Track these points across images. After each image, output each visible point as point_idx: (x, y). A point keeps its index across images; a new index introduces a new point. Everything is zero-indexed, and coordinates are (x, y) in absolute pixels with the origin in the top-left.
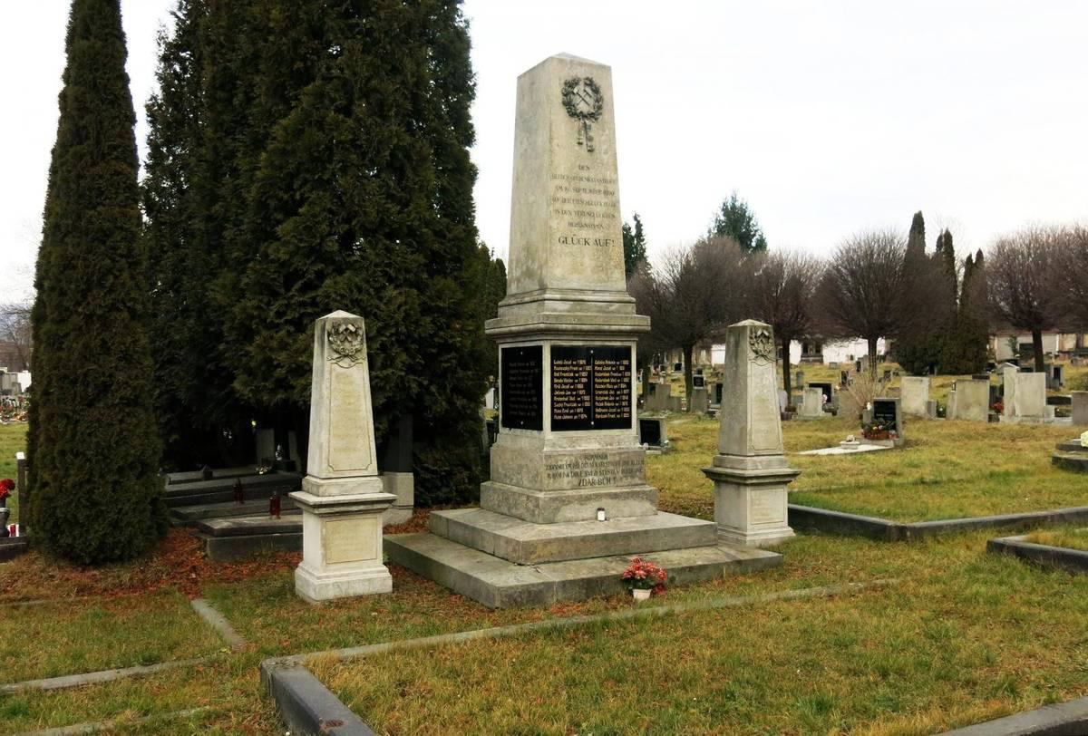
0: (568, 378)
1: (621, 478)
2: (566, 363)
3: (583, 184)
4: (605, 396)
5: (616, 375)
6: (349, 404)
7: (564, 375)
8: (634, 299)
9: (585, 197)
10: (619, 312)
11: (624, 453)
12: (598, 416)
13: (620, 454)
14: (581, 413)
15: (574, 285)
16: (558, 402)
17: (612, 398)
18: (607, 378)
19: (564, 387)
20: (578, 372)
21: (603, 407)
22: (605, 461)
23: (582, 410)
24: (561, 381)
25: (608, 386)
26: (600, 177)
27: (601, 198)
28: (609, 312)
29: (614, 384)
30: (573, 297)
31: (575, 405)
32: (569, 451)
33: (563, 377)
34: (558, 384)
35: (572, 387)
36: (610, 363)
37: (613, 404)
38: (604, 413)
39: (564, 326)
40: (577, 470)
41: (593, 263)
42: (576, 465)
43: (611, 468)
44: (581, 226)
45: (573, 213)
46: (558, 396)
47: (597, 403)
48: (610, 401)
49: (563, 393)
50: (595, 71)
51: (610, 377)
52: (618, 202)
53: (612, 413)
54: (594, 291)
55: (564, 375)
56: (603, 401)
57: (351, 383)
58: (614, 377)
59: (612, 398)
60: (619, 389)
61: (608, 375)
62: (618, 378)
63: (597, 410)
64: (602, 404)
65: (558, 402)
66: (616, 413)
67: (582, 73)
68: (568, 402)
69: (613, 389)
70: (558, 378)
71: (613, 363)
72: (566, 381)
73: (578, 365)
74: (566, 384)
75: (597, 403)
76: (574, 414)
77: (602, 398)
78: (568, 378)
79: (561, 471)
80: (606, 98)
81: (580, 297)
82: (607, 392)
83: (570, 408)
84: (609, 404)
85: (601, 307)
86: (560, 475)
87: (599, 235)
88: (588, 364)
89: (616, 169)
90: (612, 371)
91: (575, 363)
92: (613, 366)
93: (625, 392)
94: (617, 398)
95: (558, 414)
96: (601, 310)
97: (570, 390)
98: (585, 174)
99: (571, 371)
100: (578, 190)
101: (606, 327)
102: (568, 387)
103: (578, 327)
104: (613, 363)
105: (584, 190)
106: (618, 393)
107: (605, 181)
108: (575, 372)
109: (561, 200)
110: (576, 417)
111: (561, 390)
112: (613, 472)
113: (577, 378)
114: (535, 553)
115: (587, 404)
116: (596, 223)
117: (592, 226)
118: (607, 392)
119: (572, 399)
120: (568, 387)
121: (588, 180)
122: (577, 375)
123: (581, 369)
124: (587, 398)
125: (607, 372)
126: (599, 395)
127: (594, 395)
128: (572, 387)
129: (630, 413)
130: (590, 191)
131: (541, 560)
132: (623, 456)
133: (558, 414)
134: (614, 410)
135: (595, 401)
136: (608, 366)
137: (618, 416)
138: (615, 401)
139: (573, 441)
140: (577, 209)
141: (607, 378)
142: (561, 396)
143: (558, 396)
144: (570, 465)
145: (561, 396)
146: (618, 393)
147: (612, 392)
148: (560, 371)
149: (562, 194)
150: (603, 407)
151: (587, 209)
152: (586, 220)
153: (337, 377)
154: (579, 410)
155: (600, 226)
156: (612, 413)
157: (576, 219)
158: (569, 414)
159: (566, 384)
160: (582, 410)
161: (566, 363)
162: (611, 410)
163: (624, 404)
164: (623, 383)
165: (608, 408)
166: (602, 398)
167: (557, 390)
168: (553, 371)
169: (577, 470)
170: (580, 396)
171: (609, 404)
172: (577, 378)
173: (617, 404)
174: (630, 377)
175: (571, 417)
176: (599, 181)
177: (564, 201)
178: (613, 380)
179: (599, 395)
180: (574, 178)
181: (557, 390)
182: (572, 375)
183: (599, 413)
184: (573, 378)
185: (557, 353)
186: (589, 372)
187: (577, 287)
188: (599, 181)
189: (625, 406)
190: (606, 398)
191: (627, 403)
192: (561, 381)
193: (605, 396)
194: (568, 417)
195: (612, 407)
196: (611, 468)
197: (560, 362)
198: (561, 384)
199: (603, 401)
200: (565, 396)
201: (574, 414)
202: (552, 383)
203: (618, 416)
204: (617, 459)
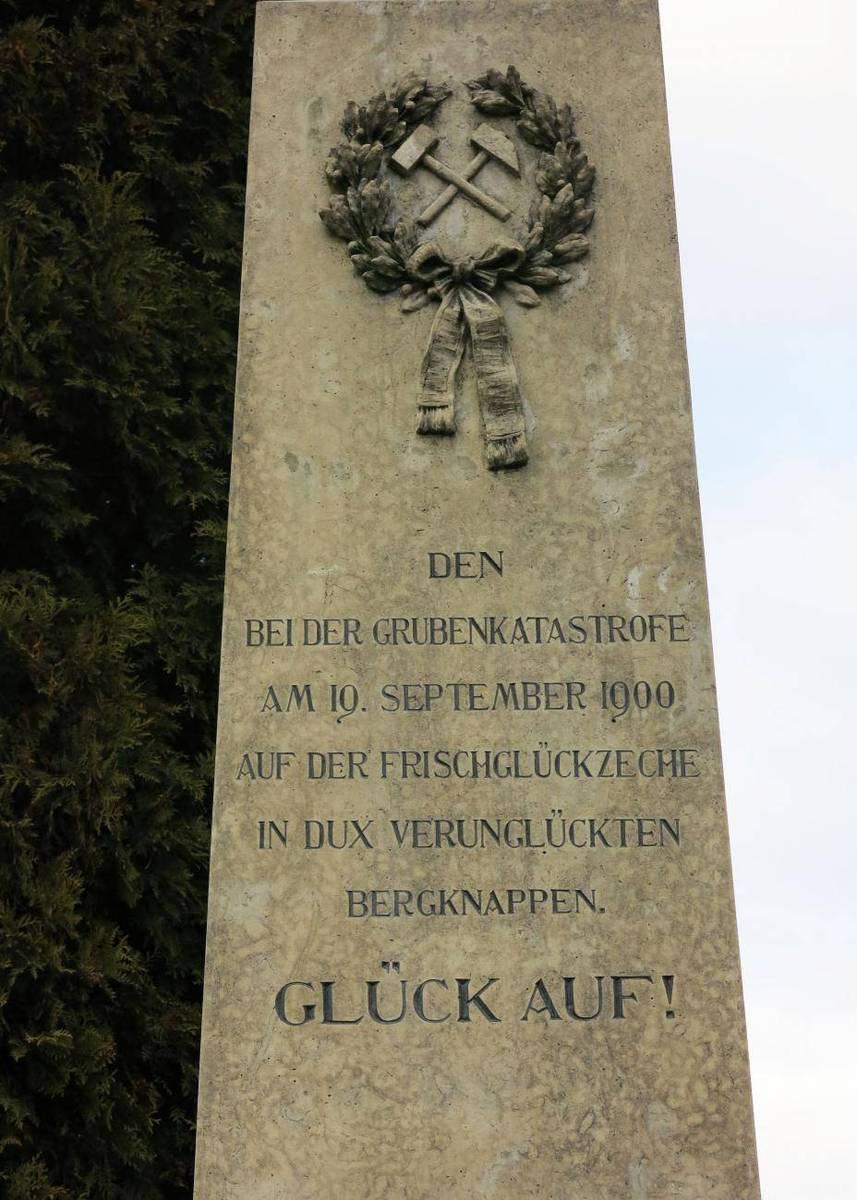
3: (450, 664)
26: (574, 603)
45: (384, 838)
52: (710, 741)
89: (691, 552)
98: (468, 599)
100: (416, 699)
105: (467, 695)
107: (612, 626)
109: (373, 766)
116: (545, 879)
121: (492, 632)
130: (506, 693)
140: (414, 807)
151: (484, 799)
152: (483, 869)
176: (571, 631)
177: (322, 766)
180: (395, 633)
188: (571, 631)
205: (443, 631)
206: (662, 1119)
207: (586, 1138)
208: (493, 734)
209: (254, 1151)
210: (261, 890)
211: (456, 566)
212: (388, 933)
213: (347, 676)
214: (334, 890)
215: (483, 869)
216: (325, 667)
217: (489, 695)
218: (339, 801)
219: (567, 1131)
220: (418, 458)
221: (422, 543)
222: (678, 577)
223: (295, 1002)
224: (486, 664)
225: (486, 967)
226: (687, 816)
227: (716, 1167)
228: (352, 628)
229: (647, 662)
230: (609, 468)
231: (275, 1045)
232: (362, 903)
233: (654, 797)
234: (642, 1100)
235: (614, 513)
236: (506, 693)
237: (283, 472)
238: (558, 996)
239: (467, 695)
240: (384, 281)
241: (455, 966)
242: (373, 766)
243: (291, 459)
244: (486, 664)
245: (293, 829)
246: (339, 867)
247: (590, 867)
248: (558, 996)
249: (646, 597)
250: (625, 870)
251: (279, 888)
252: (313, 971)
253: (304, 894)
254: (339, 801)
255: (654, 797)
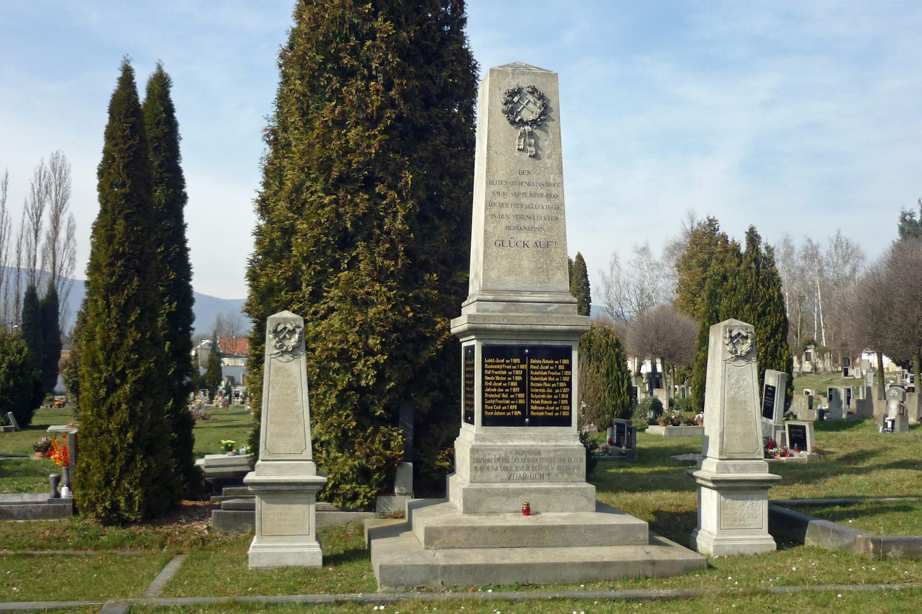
0: (500, 375)
1: (557, 475)
2: (498, 361)
3: (522, 189)
4: (542, 394)
5: (553, 373)
6: (287, 395)
7: (496, 373)
8: (576, 300)
9: (526, 201)
10: (559, 313)
11: (559, 450)
12: (533, 413)
13: (556, 451)
14: (514, 410)
15: (511, 287)
16: (489, 399)
17: (549, 397)
18: (544, 376)
19: (495, 384)
20: (511, 370)
21: (538, 405)
22: (538, 457)
23: (515, 407)
24: (492, 378)
25: (545, 384)
26: (543, 180)
27: (543, 202)
28: (547, 312)
29: (551, 382)
30: (507, 298)
31: (508, 402)
32: (500, 446)
33: (494, 375)
34: (489, 381)
35: (505, 385)
36: (547, 362)
37: (550, 402)
38: (540, 411)
39: (492, 326)
40: (507, 465)
41: (532, 265)
42: (506, 460)
43: (545, 464)
44: (519, 229)
45: (512, 218)
46: (489, 393)
47: (532, 401)
48: (548, 400)
49: (494, 390)
50: (539, 80)
51: (547, 376)
52: (563, 204)
53: (549, 411)
54: (533, 292)
55: (496, 373)
56: (540, 399)
57: (289, 376)
58: (552, 376)
59: (549, 397)
60: (559, 388)
61: (545, 373)
62: (556, 376)
63: (533, 408)
64: (538, 402)
65: (489, 399)
66: (555, 411)
67: (524, 82)
68: (501, 399)
69: (550, 388)
70: (489, 376)
71: (552, 362)
72: (498, 378)
73: (513, 364)
74: (498, 381)
75: (532, 401)
76: (506, 411)
77: (539, 396)
78: (500, 375)
79: (490, 464)
80: (551, 105)
81: (515, 298)
82: (543, 391)
83: (503, 405)
84: (546, 402)
85: (537, 307)
86: (488, 468)
87: (540, 237)
88: (523, 362)
90: (549, 369)
91: (508, 361)
92: (551, 365)
93: (565, 390)
94: (556, 397)
95: (489, 411)
96: (538, 310)
97: (502, 387)
98: (525, 178)
99: (503, 369)
100: (517, 195)
101: (540, 327)
102: (500, 384)
103: (508, 327)
104: (552, 362)
105: (525, 194)
106: (557, 391)
107: (548, 184)
108: (508, 370)
109: (510, 206)
110: (508, 414)
111: (492, 387)
112: (547, 468)
113: (510, 376)
114: (439, 539)
115: (521, 402)
116: (537, 226)
117: (532, 229)
118: (543, 391)
119: (504, 396)
120: (500, 384)
121: (529, 184)
122: (510, 373)
123: (514, 367)
124: (521, 395)
125: (544, 371)
126: (534, 393)
127: (530, 393)
128: (505, 385)
129: (570, 411)
130: (531, 195)
131: (445, 546)
132: (559, 453)
133: (489, 411)
134: (552, 408)
135: (530, 398)
136: (546, 365)
137: (557, 414)
138: (553, 400)
139: (504, 438)
140: (517, 212)
141: (544, 376)
142: (493, 393)
143: (489, 393)
144: (499, 460)
145: (493, 393)
146: (557, 391)
147: (550, 391)
148: (491, 369)
149: (500, 199)
150: (538, 405)
151: (527, 212)
152: (527, 223)
153: (276, 371)
154: (512, 407)
155: (541, 228)
156: (549, 411)
157: (514, 222)
158: (501, 411)
159: (498, 381)
160: (515, 407)
161: (498, 361)
162: (548, 408)
163: (563, 402)
164: (562, 381)
165: (545, 405)
166: (539, 396)
167: (488, 387)
168: (483, 369)
169: (507, 465)
170: (513, 393)
171: (546, 402)
172: (510, 376)
173: (555, 403)
174: (570, 377)
175: (504, 413)
177: (502, 205)
178: (550, 379)
179: (534, 393)
180: (513, 183)
181: (488, 387)
182: (505, 372)
183: (535, 411)
184: (507, 376)
185: (488, 352)
186: (524, 370)
187: (515, 289)
189: (565, 405)
190: (543, 396)
191: (566, 402)
192: (492, 378)
193: (542, 394)
194: (501, 414)
195: (550, 405)
196: (545, 464)
197: (491, 361)
198: (493, 381)
199: (540, 399)
200: (497, 393)
201: (506, 411)
202: (483, 380)
203: (557, 414)
204: (552, 455)
205: (521, 184)
206: (554, 265)
207: (542, 267)
208: (529, 201)
209: (491, 267)
210: (492, 225)
211: (523, 172)
212: (512, 233)
213: (506, 191)
214: (504, 226)
215: (527, 223)
216: (502, 189)
217: (528, 195)
218: (505, 211)
219: (540, 265)
220: (517, 154)
221: (517, 168)
222: (559, 177)
223: (498, 243)
224: (528, 190)
225: (527, 239)
226: (559, 216)
227: (562, 272)
228: (506, 182)
229: (554, 191)
230: (549, 157)
231: (495, 250)
232: (508, 228)
233: (554, 213)
234: (551, 261)
235: (549, 165)
236: (531, 195)
237: (495, 155)
238: (538, 244)
239: (525, 194)
240: (513, 123)
241: (523, 239)
242: (510, 206)
243: (496, 153)
244: (528, 190)
245: (497, 215)
246: (504, 222)
247: (544, 224)
248: (538, 244)
249: (554, 179)
250: (550, 225)
251: (495, 225)
252: (500, 239)
253: (499, 226)
254: (505, 211)
255: (554, 213)
